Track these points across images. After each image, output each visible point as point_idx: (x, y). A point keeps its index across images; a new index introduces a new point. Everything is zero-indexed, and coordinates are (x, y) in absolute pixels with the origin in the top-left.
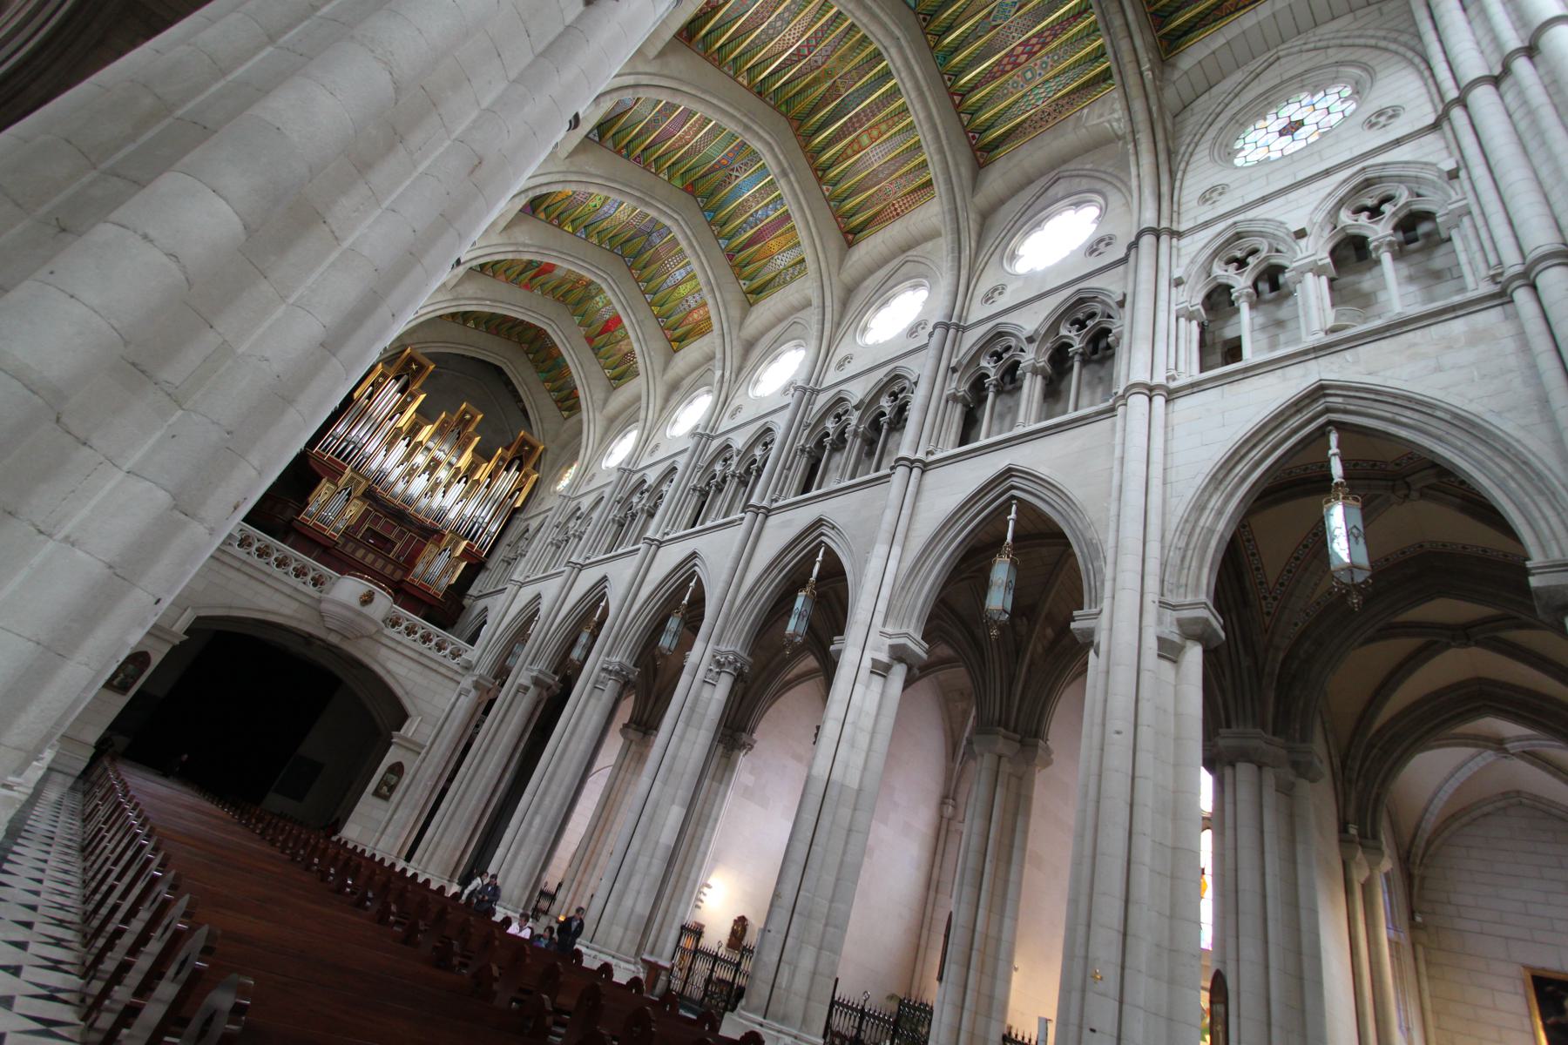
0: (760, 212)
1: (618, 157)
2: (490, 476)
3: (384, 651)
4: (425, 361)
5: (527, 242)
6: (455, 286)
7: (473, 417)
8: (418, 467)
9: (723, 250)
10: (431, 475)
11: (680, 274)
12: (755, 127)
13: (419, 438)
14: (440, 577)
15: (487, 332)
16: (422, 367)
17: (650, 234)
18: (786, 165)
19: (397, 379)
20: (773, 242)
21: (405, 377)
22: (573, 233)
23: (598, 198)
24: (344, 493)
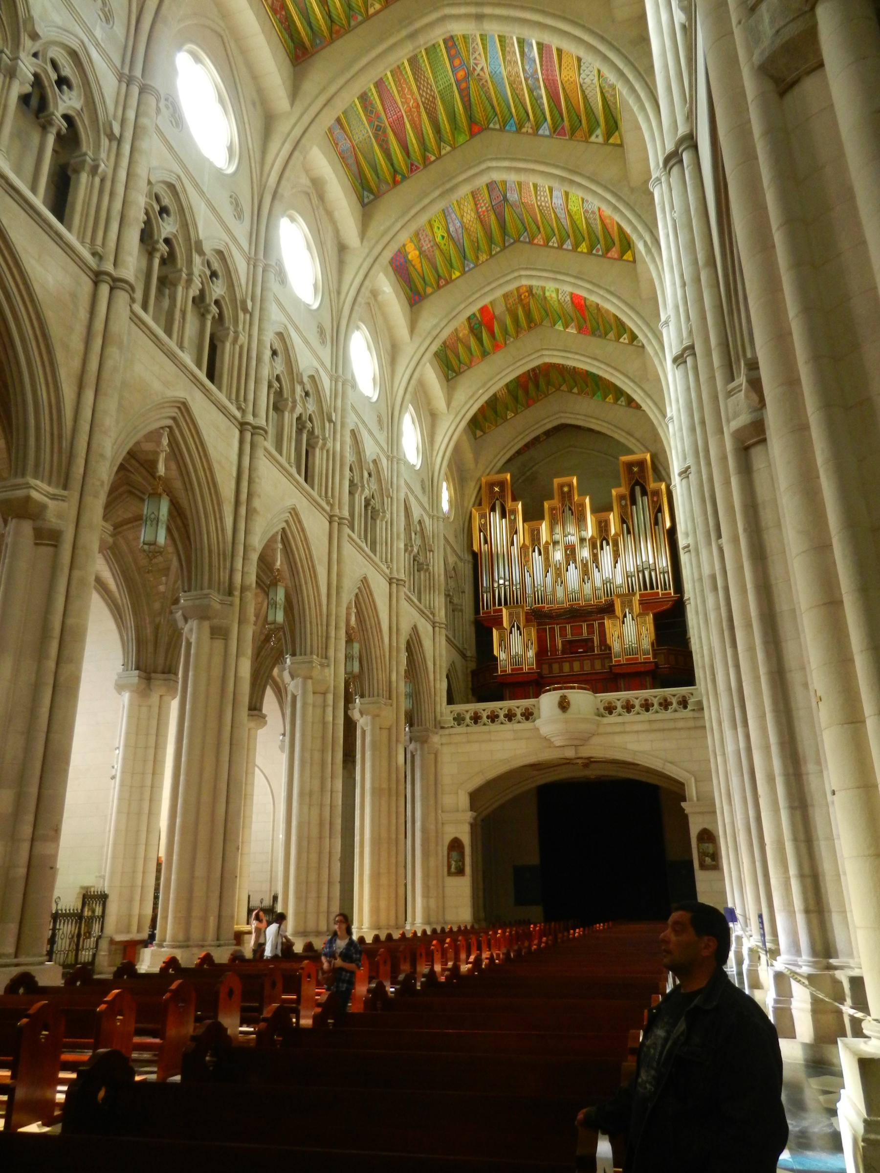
0: (527, 67)
1: (399, 187)
2: (623, 521)
3: (618, 740)
4: (500, 477)
5: (434, 323)
6: (448, 405)
7: (570, 485)
8: (560, 564)
9: (550, 136)
10: (575, 561)
11: (557, 198)
12: (418, 25)
13: (544, 536)
14: (639, 640)
15: (526, 409)
16: (502, 484)
17: (505, 199)
18: (472, 10)
19: (493, 509)
20: (564, 73)
21: (498, 503)
22: (463, 273)
23: (435, 229)
24: (515, 630)
